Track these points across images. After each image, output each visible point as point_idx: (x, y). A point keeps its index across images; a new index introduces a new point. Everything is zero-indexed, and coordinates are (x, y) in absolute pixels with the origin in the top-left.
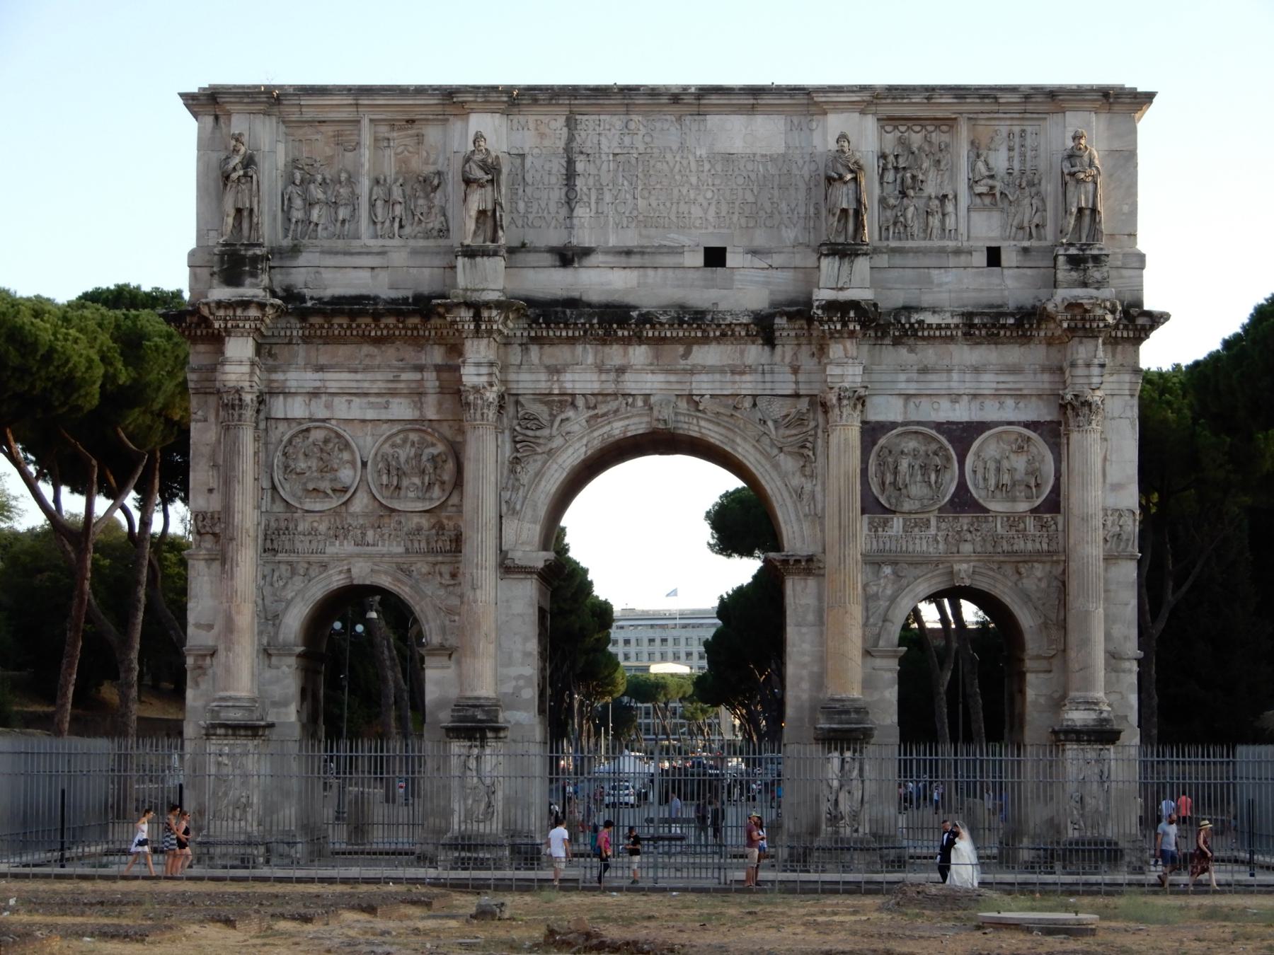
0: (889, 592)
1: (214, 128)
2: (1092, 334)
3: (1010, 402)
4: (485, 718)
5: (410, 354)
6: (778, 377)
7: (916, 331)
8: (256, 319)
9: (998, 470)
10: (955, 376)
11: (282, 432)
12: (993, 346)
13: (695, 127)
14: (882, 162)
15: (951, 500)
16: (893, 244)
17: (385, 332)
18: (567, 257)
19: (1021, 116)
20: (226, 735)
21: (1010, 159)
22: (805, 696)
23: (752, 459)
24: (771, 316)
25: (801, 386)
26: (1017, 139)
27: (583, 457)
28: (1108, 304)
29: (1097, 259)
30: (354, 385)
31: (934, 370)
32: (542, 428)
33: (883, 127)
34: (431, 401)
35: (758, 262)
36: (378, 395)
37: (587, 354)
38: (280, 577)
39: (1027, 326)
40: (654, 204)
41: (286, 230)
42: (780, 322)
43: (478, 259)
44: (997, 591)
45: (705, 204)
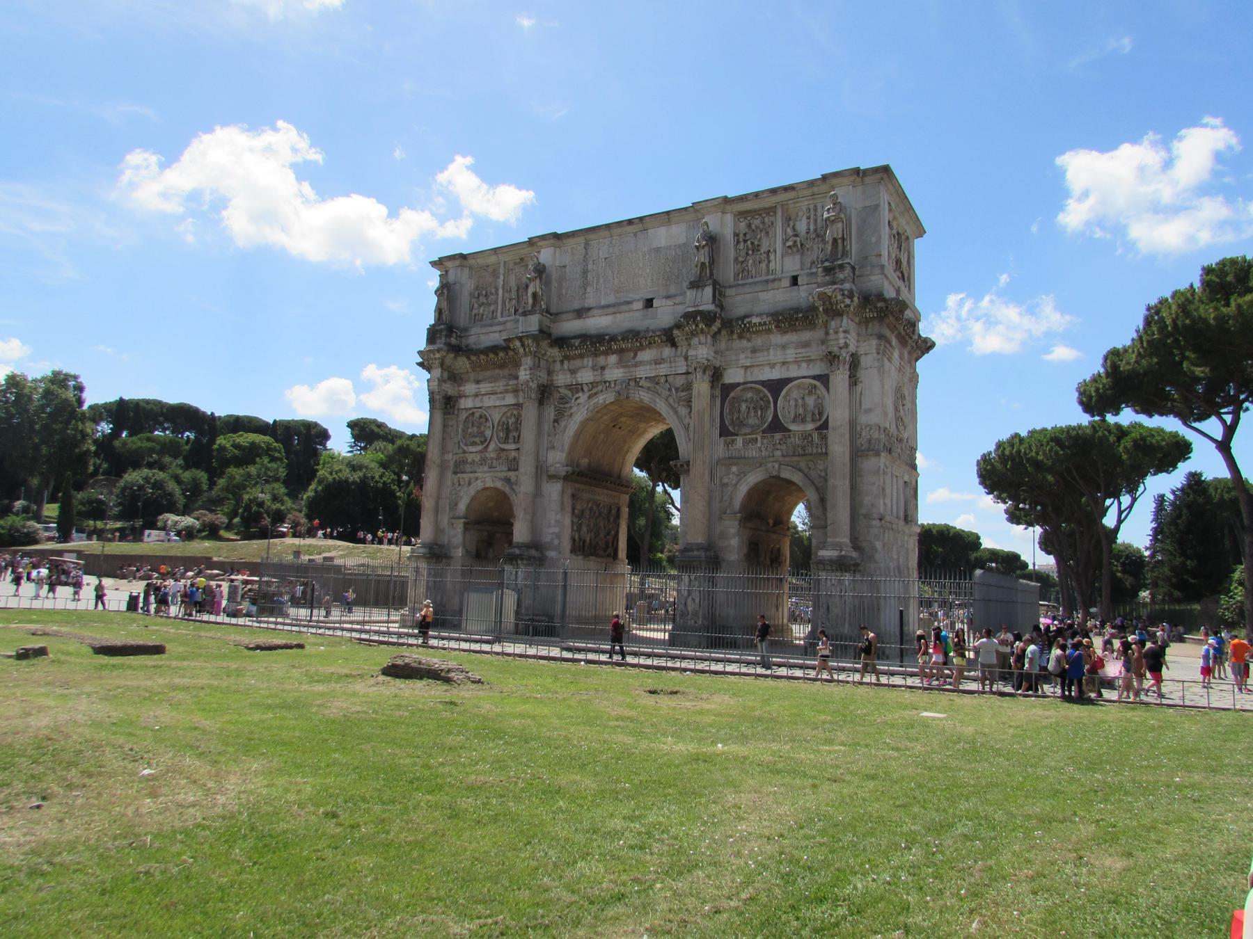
2: (839, 314)
3: (804, 365)
6: (677, 364)
7: (748, 330)
9: (796, 405)
10: (771, 352)
11: (464, 415)
15: (769, 426)
16: (740, 282)
18: (580, 313)
21: (808, 224)
24: (671, 329)
26: (812, 212)
28: (846, 292)
29: (841, 267)
31: (760, 351)
35: (670, 302)
37: (589, 361)
42: (676, 332)
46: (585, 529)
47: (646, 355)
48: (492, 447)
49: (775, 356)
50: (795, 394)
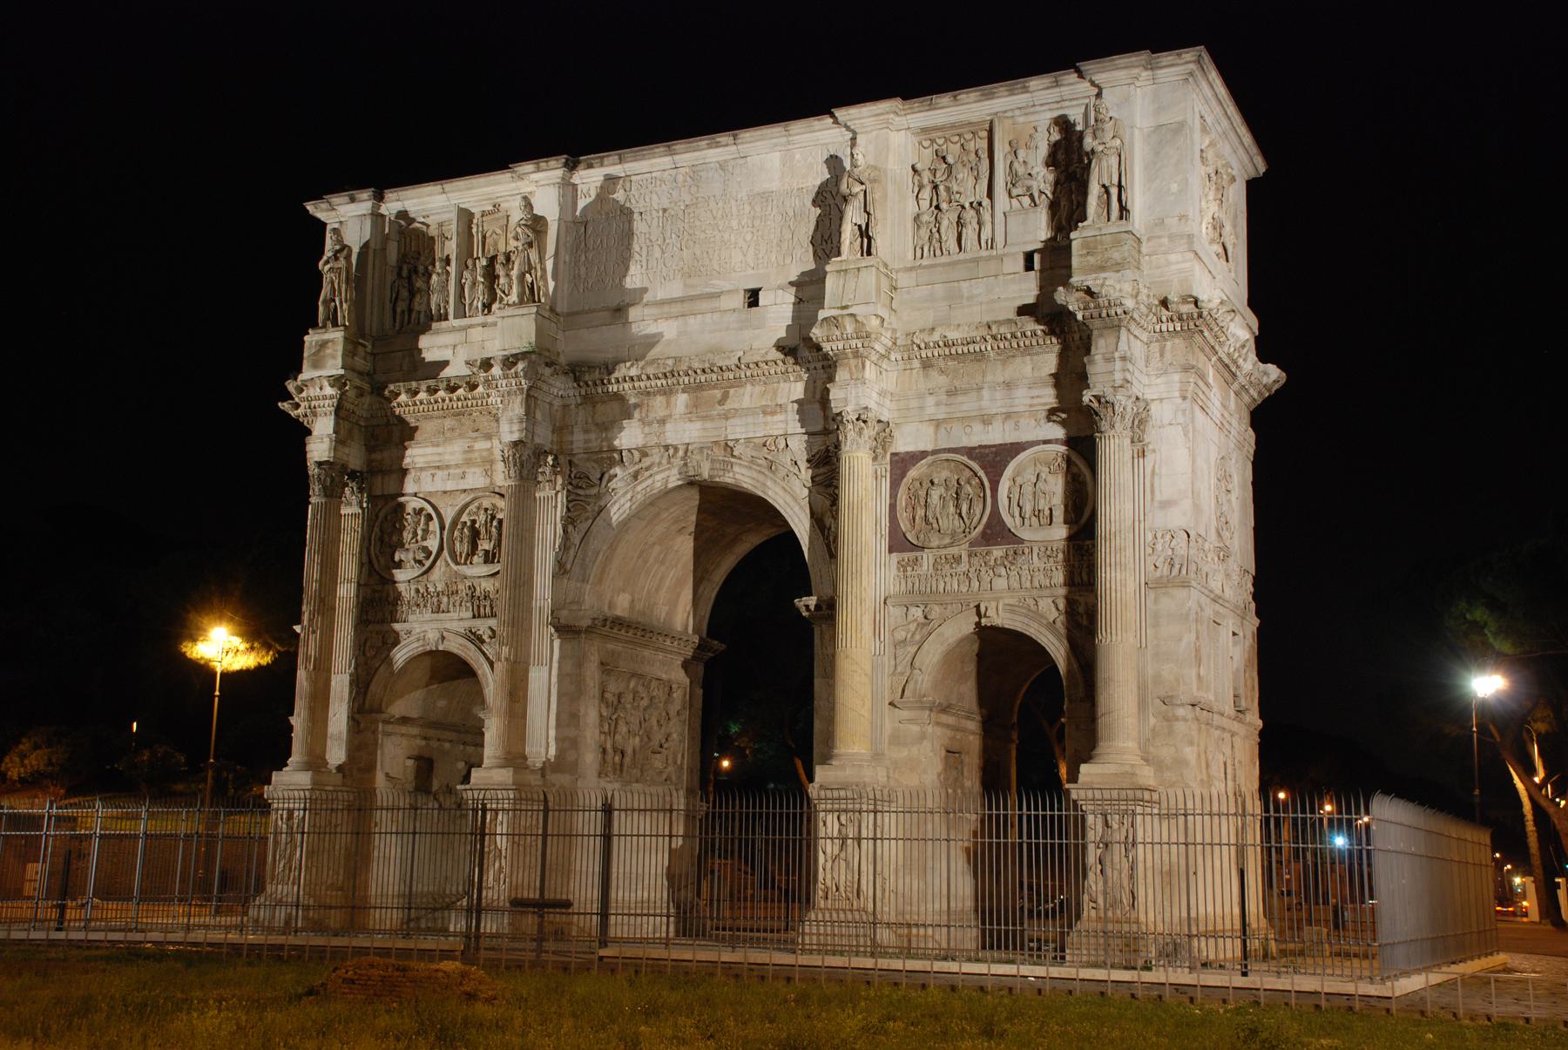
0: (917, 637)
5: (485, 423)
8: (332, 397)
10: (986, 393)
14: (917, 178)
15: (984, 534)
17: (460, 404)
19: (1059, 105)
23: (781, 502)
27: (628, 512)
30: (437, 458)
31: (965, 392)
32: (592, 486)
33: (920, 143)
40: (698, 253)
44: (1032, 631)
45: (745, 247)
46: (623, 729)
47: (747, 396)
48: (438, 574)
49: (991, 401)
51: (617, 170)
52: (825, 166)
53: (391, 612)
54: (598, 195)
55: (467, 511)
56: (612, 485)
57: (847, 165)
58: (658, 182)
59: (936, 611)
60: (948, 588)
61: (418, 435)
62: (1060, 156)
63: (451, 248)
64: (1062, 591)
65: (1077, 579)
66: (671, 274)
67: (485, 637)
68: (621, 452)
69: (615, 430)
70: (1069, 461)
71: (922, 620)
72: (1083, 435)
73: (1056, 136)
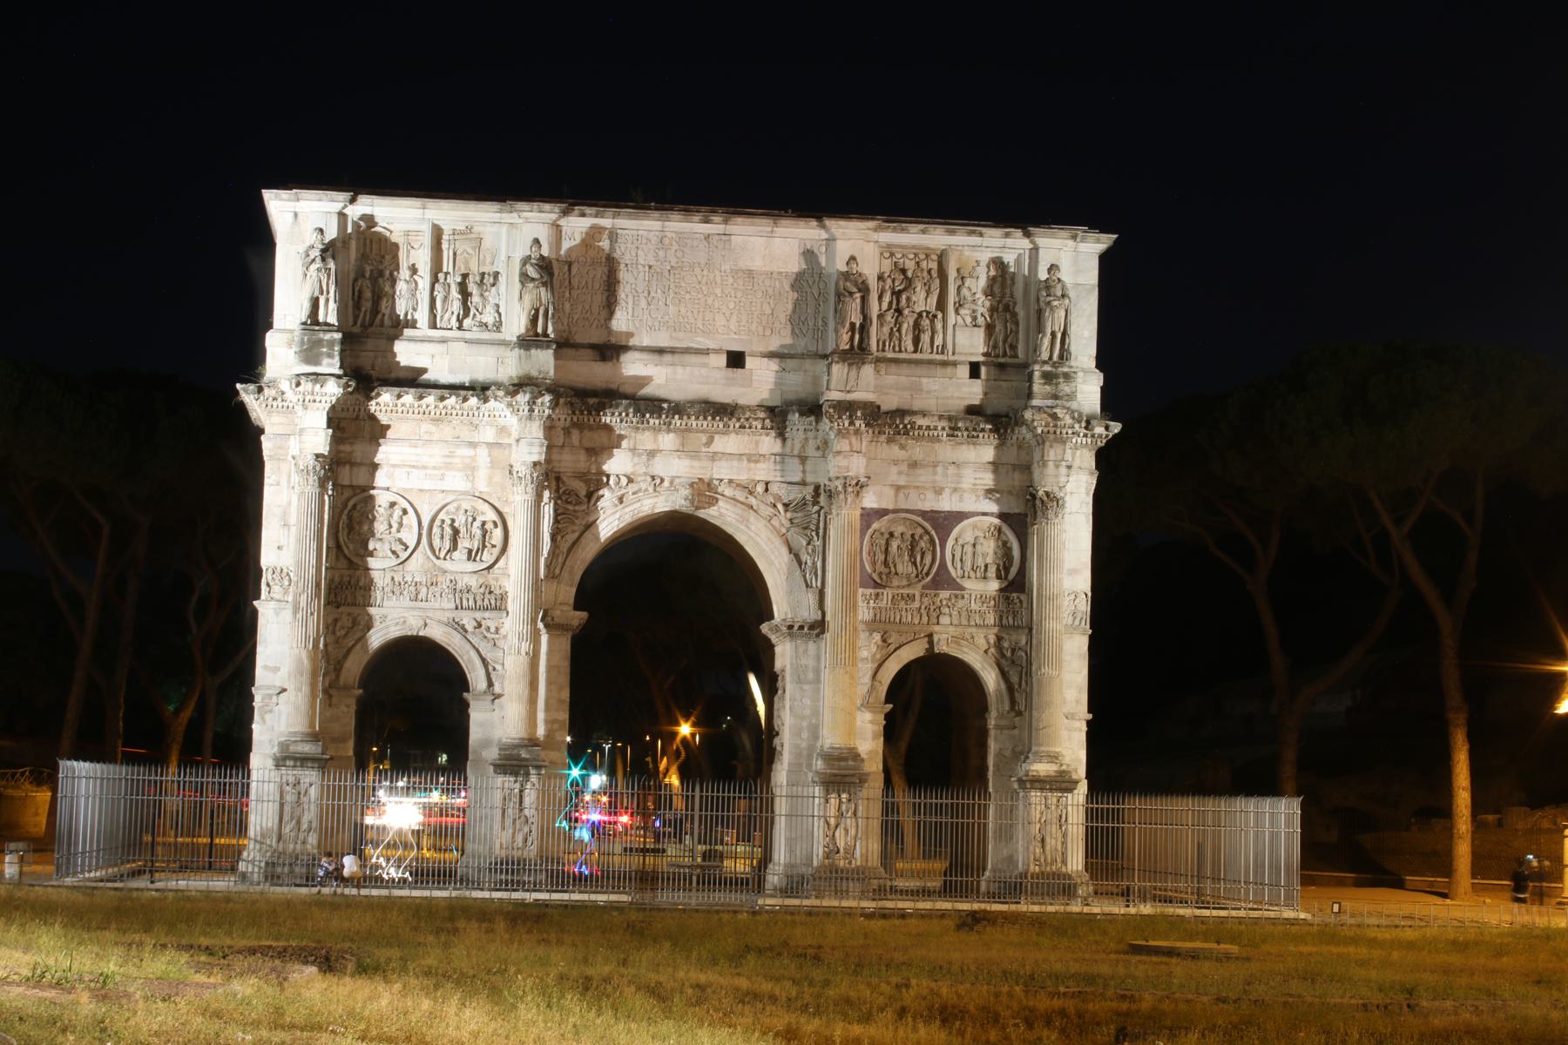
0: (878, 656)
1: (293, 224)
4: (528, 756)
5: (466, 434)
9: (974, 554)
10: (939, 469)
12: (972, 447)
13: (721, 245)
14: (881, 283)
15: (934, 579)
17: (444, 412)
20: (295, 766)
22: (804, 745)
25: (807, 475)
27: (615, 529)
28: (1076, 415)
29: (1067, 376)
32: (579, 503)
33: (882, 254)
34: (483, 473)
36: (435, 468)
38: (343, 628)
39: (1002, 431)
40: (683, 311)
41: (356, 318)
43: (533, 351)
45: (728, 314)
47: (730, 442)
50: (969, 537)
51: (606, 223)
52: (802, 258)
53: (364, 596)
54: (583, 240)
55: (445, 510)
56: (600, 504)
57: (823, 261)
58: (644, 241)
59: (894, 639)
60: (904, 620)
61: (390, 434)
62: (997, 289)
63: (423, 258)
64: (996, 630)
65: (1004, 622)
66: (657, 324)
67: (470, 628)
68: (608, 476)
69: (605, 456)
70: (1000, 531)
71: (880, 643)
72: (1012, 512)
73: (992, 273)
